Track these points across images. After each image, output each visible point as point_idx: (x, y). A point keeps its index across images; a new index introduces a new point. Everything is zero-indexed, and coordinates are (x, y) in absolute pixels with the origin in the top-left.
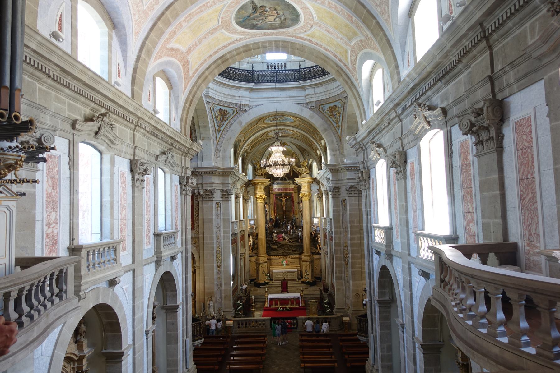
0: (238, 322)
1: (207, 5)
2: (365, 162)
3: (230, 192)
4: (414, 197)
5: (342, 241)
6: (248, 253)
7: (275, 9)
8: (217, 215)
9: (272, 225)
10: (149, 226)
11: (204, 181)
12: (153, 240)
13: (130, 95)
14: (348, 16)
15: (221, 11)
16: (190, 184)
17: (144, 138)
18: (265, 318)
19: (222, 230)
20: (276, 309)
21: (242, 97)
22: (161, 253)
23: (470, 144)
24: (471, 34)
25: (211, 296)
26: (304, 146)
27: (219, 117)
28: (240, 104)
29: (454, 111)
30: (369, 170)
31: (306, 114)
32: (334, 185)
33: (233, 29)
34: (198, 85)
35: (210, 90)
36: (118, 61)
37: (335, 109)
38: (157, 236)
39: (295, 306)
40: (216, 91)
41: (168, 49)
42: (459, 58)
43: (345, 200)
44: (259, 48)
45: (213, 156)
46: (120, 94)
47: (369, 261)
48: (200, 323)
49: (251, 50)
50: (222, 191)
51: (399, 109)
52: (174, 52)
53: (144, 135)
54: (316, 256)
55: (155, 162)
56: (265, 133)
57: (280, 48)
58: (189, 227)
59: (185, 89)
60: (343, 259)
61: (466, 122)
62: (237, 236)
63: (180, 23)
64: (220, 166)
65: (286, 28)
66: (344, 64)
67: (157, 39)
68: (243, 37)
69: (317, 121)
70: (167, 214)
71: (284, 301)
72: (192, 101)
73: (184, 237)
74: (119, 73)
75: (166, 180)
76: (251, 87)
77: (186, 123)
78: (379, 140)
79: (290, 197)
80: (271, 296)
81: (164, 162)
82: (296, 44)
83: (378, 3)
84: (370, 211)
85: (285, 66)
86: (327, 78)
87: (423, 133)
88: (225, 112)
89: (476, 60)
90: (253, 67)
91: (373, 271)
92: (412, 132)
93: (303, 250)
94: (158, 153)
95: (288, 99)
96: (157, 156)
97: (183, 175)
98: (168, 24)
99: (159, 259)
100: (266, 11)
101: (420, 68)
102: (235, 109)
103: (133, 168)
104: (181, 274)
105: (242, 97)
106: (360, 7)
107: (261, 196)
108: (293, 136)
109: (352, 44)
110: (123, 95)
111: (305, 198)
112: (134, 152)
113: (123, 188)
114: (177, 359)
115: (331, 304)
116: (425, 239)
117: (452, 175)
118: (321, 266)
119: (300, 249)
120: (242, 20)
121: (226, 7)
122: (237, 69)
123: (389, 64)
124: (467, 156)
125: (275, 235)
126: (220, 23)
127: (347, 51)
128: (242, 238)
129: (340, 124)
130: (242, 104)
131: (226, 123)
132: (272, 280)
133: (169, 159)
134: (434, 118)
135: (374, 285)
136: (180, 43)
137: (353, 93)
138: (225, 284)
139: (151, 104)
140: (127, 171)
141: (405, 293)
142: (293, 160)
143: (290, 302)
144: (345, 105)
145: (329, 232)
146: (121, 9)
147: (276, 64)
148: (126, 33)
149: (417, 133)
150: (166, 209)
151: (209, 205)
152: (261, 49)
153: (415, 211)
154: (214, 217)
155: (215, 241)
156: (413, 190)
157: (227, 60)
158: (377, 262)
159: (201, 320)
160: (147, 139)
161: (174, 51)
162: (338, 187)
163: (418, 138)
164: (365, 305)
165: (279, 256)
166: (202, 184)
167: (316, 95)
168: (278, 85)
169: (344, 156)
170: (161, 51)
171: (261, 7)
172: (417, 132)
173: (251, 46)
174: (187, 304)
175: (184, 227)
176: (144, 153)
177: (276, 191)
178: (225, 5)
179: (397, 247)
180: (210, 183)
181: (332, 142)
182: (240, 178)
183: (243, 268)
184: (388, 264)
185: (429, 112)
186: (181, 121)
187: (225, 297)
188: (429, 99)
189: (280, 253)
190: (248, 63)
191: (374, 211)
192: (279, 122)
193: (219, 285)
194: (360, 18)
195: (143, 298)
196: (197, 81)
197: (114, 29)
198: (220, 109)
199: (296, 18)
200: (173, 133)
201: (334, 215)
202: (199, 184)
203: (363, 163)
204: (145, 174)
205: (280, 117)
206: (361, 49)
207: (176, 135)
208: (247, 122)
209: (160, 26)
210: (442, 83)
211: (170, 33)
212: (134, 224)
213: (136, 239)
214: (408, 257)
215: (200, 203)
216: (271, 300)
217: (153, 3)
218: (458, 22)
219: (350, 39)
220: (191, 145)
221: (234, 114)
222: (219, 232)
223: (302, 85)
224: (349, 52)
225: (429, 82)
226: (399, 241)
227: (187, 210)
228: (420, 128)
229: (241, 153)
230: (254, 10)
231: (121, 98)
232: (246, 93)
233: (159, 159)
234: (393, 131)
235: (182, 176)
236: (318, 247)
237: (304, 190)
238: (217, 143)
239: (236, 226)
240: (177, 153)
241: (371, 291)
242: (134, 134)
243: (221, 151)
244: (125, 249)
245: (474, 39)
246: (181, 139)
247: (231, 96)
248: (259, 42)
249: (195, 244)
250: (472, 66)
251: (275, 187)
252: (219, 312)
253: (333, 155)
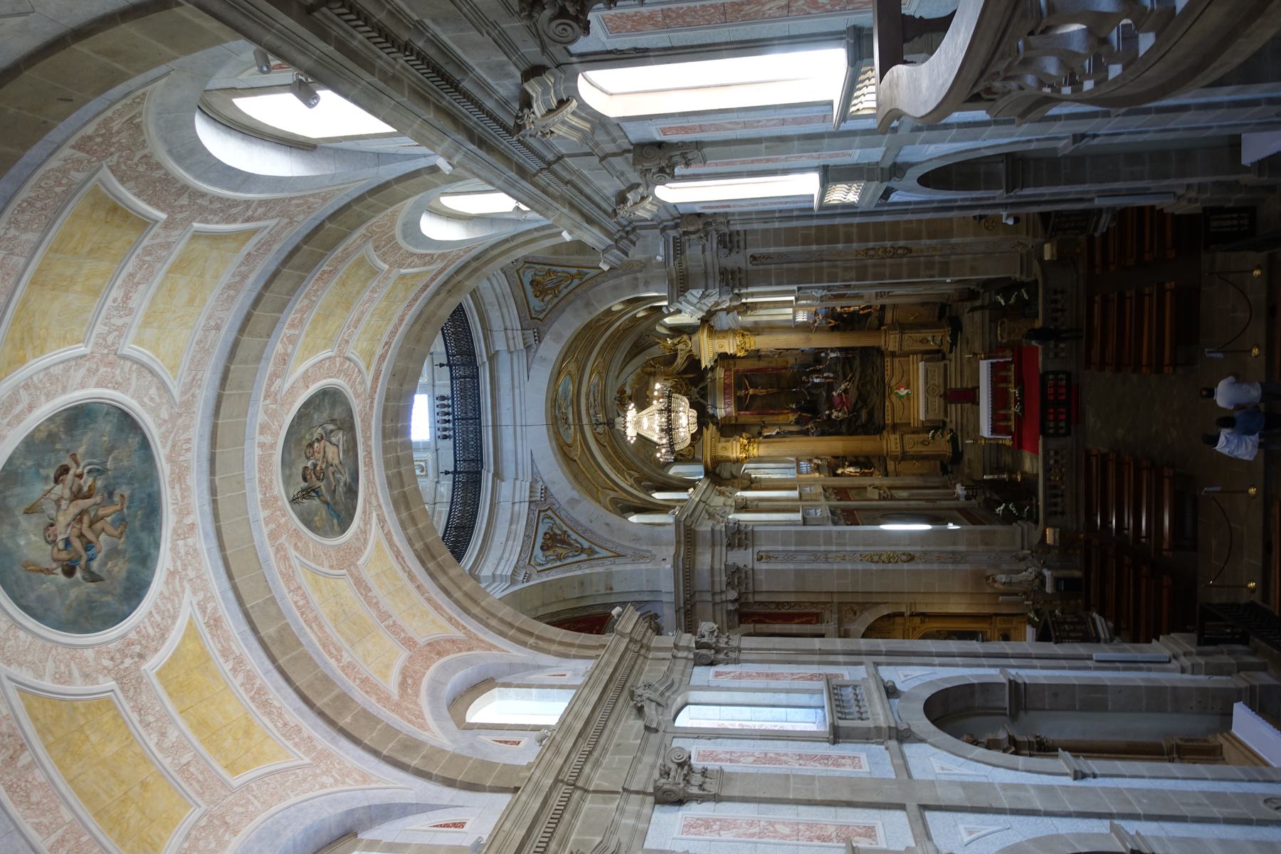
0: (1048, 515)
1: (303, 606)
2: (661, 226)
3: (733, 528)
4: (746, 125)
5: (854, 264)
6: (878, 480)
7: (311, 445)
8: (785, 561)
9: (811, 419)
10: (813, 758)
11: (707, 587)
12: (848, 746)
13: (506, 798)
14: (320, 282)
15: (315, 572)
16: (714, 640)
17: (605, 762)
18: (1040, 450)
19: (823, 548)
20: (1019, 420)
21: (514, 498)
22: (878, 729)
23: (612, 12)
24: (336, 31)
25: (981, 579)
26: (626, 345)
27: (559, 551)
28: (530, 502)
29: (531, 51)
30: (682, 216)
31: (551, 349)
32: (717, 285)
33: (358, 539)
34: (483, 616)
35: (498, 572)
36: (424, 828)
37: (539, 283)
38: (836, 735)
39: (1012, 374)
40: (501, 558)
41: (401, 696)
42: (399, 51)
43: (753, 257)
44: (400, 474)
45: (650, 566)
46: (501, 836)
47: (906, 212)
48: (1053, 622)
49: (404, 493)
50: (730, 546)
51: (533, 165)
52: (410, 681)
53: (597, 764)
54: (889, 317)
55: (661, 733)
56: (597, 440)
57: (399, 425)
58: (817, 643)
59: (495, 647)
60: (898, 260)
61: (555, 28)
62: (836, 507)
63: (343, 669)
64: (672, 550)
65: (352, 417)
66: (433, 279)
67: (379, 727)
68: (374, 514)
69: (569, 325)
70: (785, 703)
71: (999, 399)
72: (520, 630)
73: (841, 658)
74: (455, 825)
75: (703, 700)
76: (490, 475)
77: (572, 645)
78: (608, 198)
79: (746, 376)
80: (985, 430)
81: (660, 709)
82: (388, 389)
83: (286, 220)
84: (781, 211)
85: (443, 398)
86: (469, 305)
87: (588, 114)
88: (548, 536)
89: (400, 11)
90: (447, 473)
91: (932, 202)
92: (585, 137)
93: (872, 348)
94: (639, 724)
95: (517, 391)
96: (647, 728)
97: (691, 656)
98: (344, 700)
99: (894, 733)
100: (315, 465)
101: (427, 134)
102: (542, 514)
103: (675, 798)
104: (928, 670)
105: (514, 498)
106: (296, 260)
107: (743, 447)
108: (604, 373)
109: (386, 267)
110: (504, 828)
111: (747, 345)
112: (638, 792)
113: (721, 829)
114: (1146, 687)
115: (1008, 286)
116: (854, 102)
117: (692, 47)
118: (913, 305)
119: (871, 357)
120: (335, 521)
121: (308, 562)
122: (451, 509)
123: (427, 187)
124: (643, 16)
125: (835, 414)
126: (344, 571)
127: (403, 277)
128: (842, 493)
129: (574, 271)
130: (531, 497)
131: (574, 536)
132: (944, 423)
133: (653, 696)
134: (549, 93)
135: (966, 200)
136: (388, 667)
137: (500, 255)
138: (954, 544)
139: (526, 739)
140: (680, 813)
141: (992, 137)
142: (658, 386)
143: (1002, 385)
144: (530, 260)
145: (829, 291)
146: (309, 822)
147: (439, 418)
148: (363, 808)
149: (588, 125)
150: (772, 703)
151: (762, 577)
152: (403, 469)
153: (784, 122)
154: (792, 567)
155: (849, 567)
156: (731, 126)
157: (427, 547)
158: (906, 193)
159: (1046, 620)
160: (606, 754)
161: (408, 681)
162: (721, 273)
163: (599, 121)
164: (1017, 220)
165: (887, 404)
166: (714, 594)
168: (487, 418)
169: (649, 260)
170: (406, 713)
171: (305, 479)
172: (585, 126)
173: (395, 492)
174: (1005, 656)
175: (817, 658)
176: (640, 766)
177: (731, 410)
178: (303, 565)
179: (874, 154)
180: (712, 576)
181: (615, 288)
182: (700, 500)
183: (915, 491)
184: (913, 175)
185: (535, 106)
186: (566, 656)
187: (986, 544)
188: (504, 104)
189: (878, 403)
190: (437, 482)
191: (780, 203)
192: (570, 409)
193: (956, 558)
194: (322, 256)
195: (991, 785)
196: (475, 617)
197: (356, 835)
198: (542, 548)
199: (329, 397)
200: (593, 687)
201: (789, 283)
202: (714, 599)
203: (663, 230)
204: (690, 766)
205: (560, 408)
206: (397, 247)
207: (598, 678)
208: (570, 486)
209: (348, 719)
210: (463, 80)
211: (367, 692)
212: (809, 800)
213: (846, 796)
214: (899, 133)
215: (758, 598)
216: (994, 430)
217: (297, 740)
218: (308, 63)
219: (374, 272)
220: (622, 635)
221: (553, 516)
222: (826, 556)
223: (485, 359)
224: (403, 271)
225: (463, 109)
226: (858, 151)
227: (774, 649)
228: (575, 121)
229: (642, 495)
230: (313, 494)
231: (509, 833)
232: (505, 489)
233: (654, 725)
234: (585, 172)
235: (695, 659)
236: (866, 311)
237: (730, 346)
238: (619, 556)
239: (812, 511)
240: (640, 672)
241: (982, 207)
242: (595, 792)
243: (637, 546)
244: (870, 832)
245: (347, 21)
246: (607, 664)
247: (511, 523)
248: (387, 477)
249: (855, 613)
250: (416, 18)
251: (721, 413)
252: (1024, 558)
253: (647, 285)
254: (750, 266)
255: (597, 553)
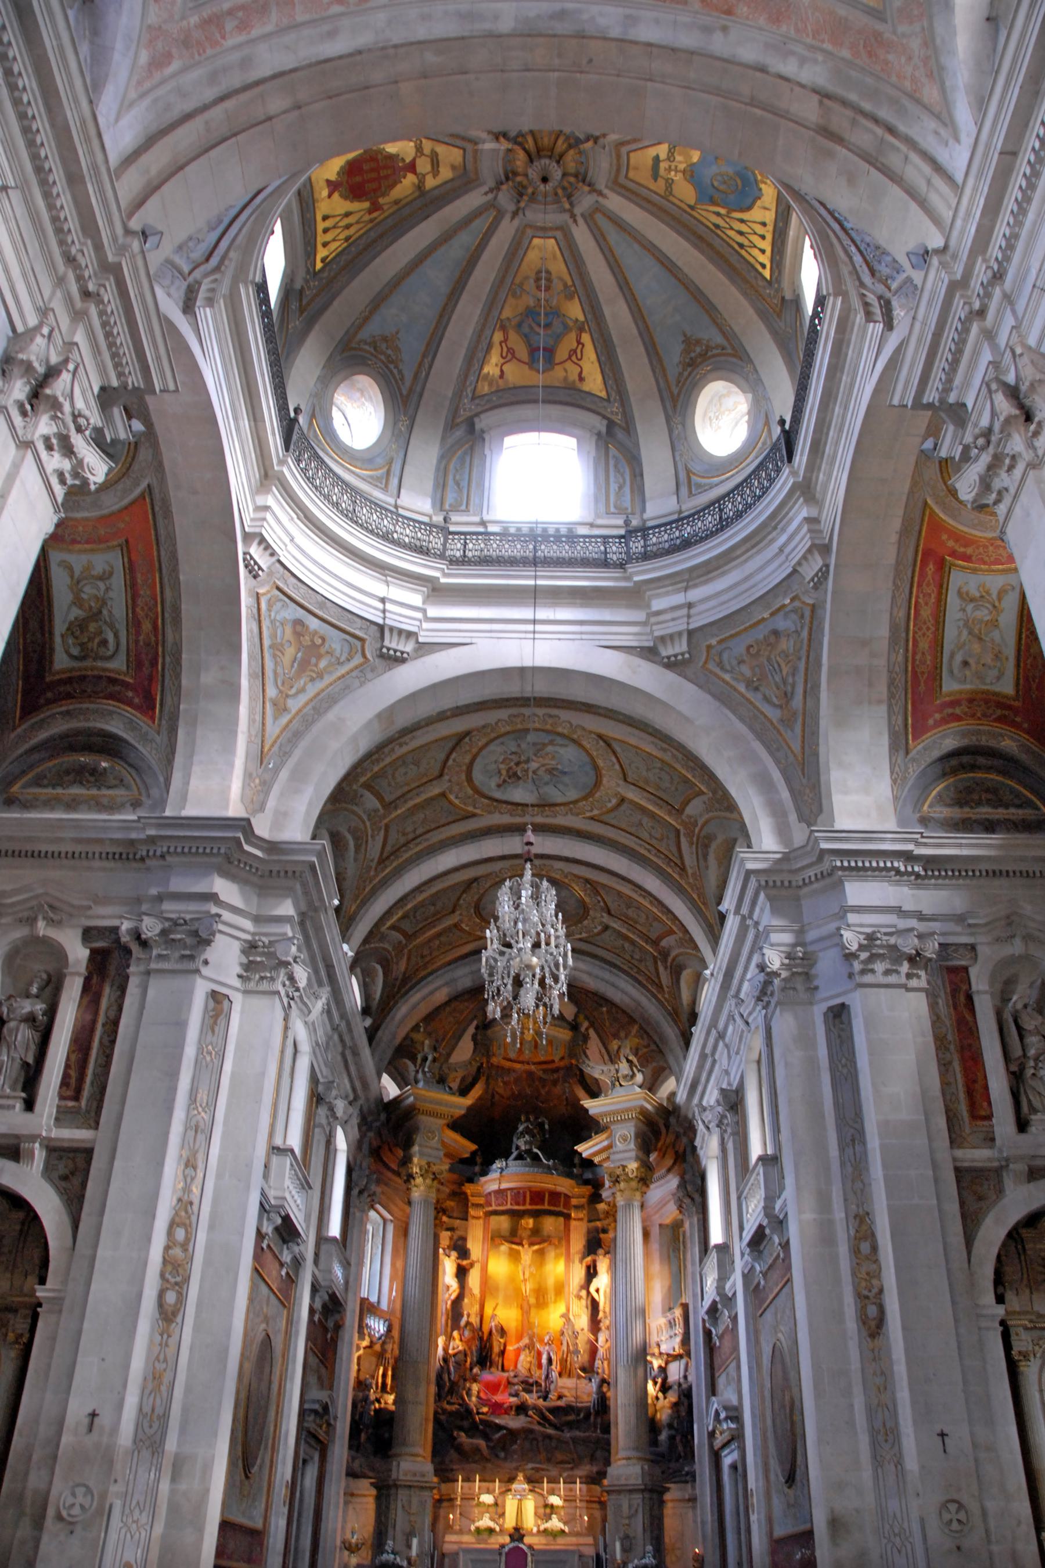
27: (290, 651)
28: (381, 628)
50: (251, 947)
102: (358, 644)
129: (797, 702)
130: (392, 629)
166: (160, 898)
167: (693, 611)
198: (298, 622)
249: (65, 1178)
254: (824, 1007)
255: (276, 718)
